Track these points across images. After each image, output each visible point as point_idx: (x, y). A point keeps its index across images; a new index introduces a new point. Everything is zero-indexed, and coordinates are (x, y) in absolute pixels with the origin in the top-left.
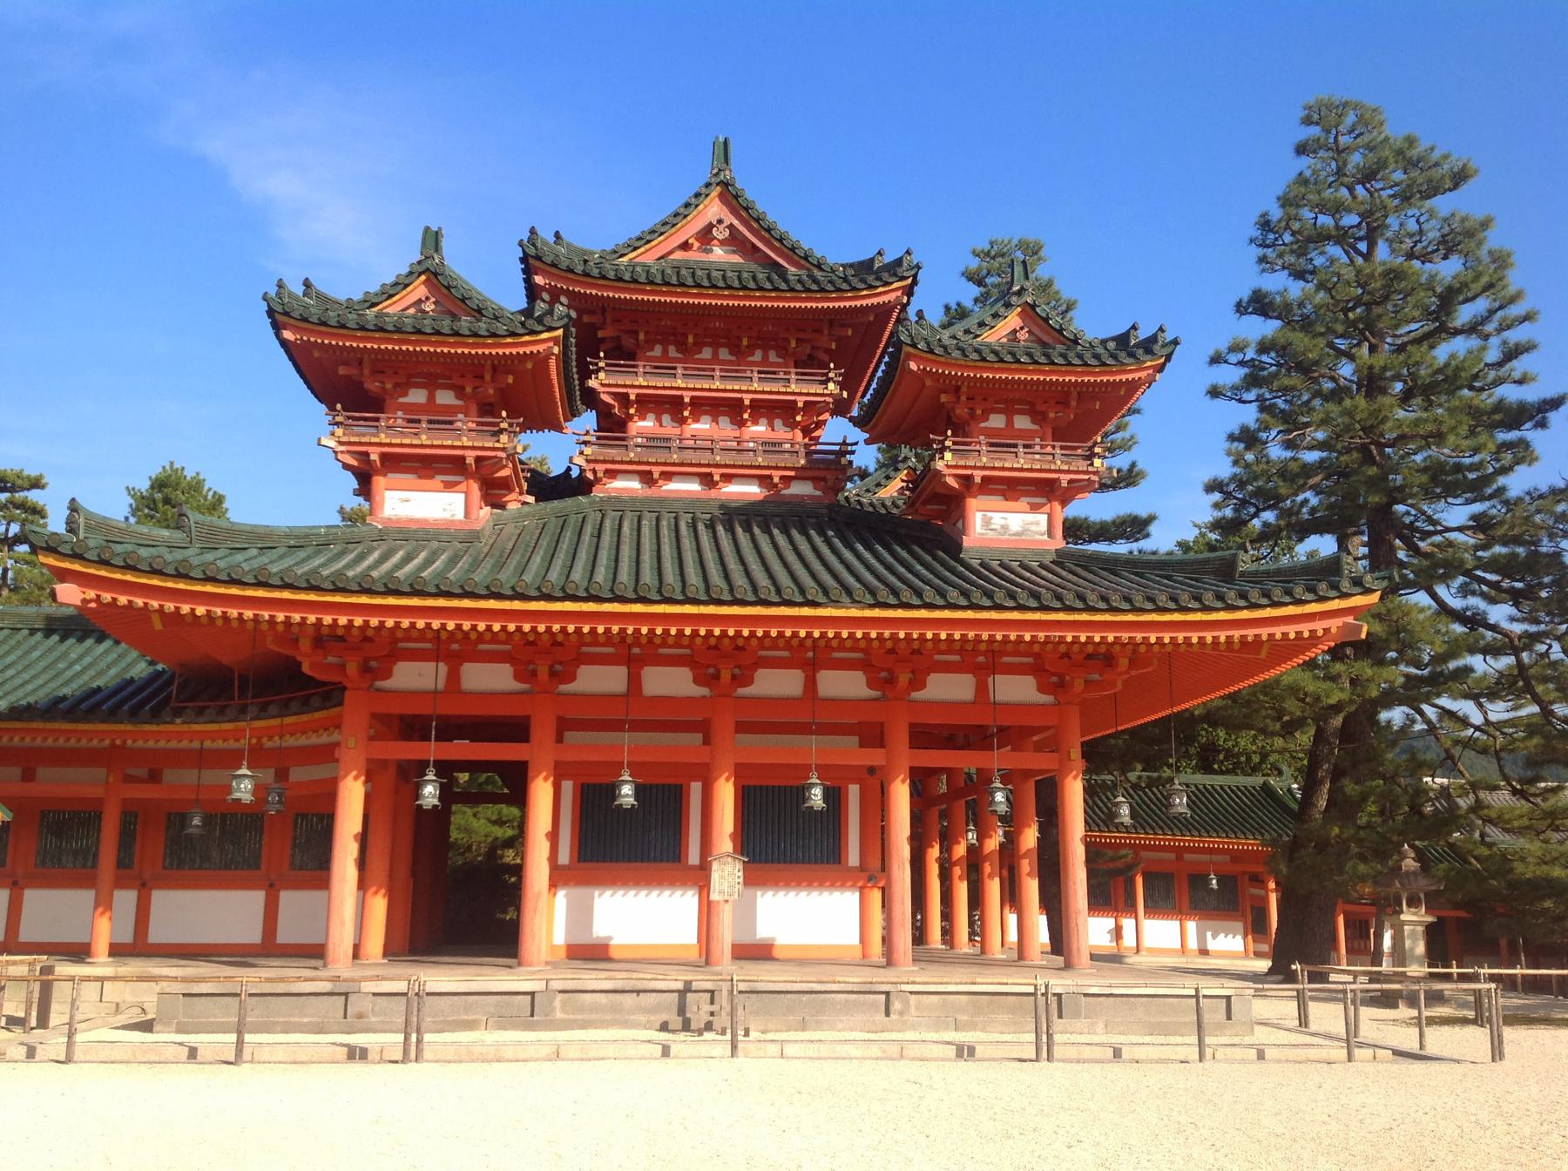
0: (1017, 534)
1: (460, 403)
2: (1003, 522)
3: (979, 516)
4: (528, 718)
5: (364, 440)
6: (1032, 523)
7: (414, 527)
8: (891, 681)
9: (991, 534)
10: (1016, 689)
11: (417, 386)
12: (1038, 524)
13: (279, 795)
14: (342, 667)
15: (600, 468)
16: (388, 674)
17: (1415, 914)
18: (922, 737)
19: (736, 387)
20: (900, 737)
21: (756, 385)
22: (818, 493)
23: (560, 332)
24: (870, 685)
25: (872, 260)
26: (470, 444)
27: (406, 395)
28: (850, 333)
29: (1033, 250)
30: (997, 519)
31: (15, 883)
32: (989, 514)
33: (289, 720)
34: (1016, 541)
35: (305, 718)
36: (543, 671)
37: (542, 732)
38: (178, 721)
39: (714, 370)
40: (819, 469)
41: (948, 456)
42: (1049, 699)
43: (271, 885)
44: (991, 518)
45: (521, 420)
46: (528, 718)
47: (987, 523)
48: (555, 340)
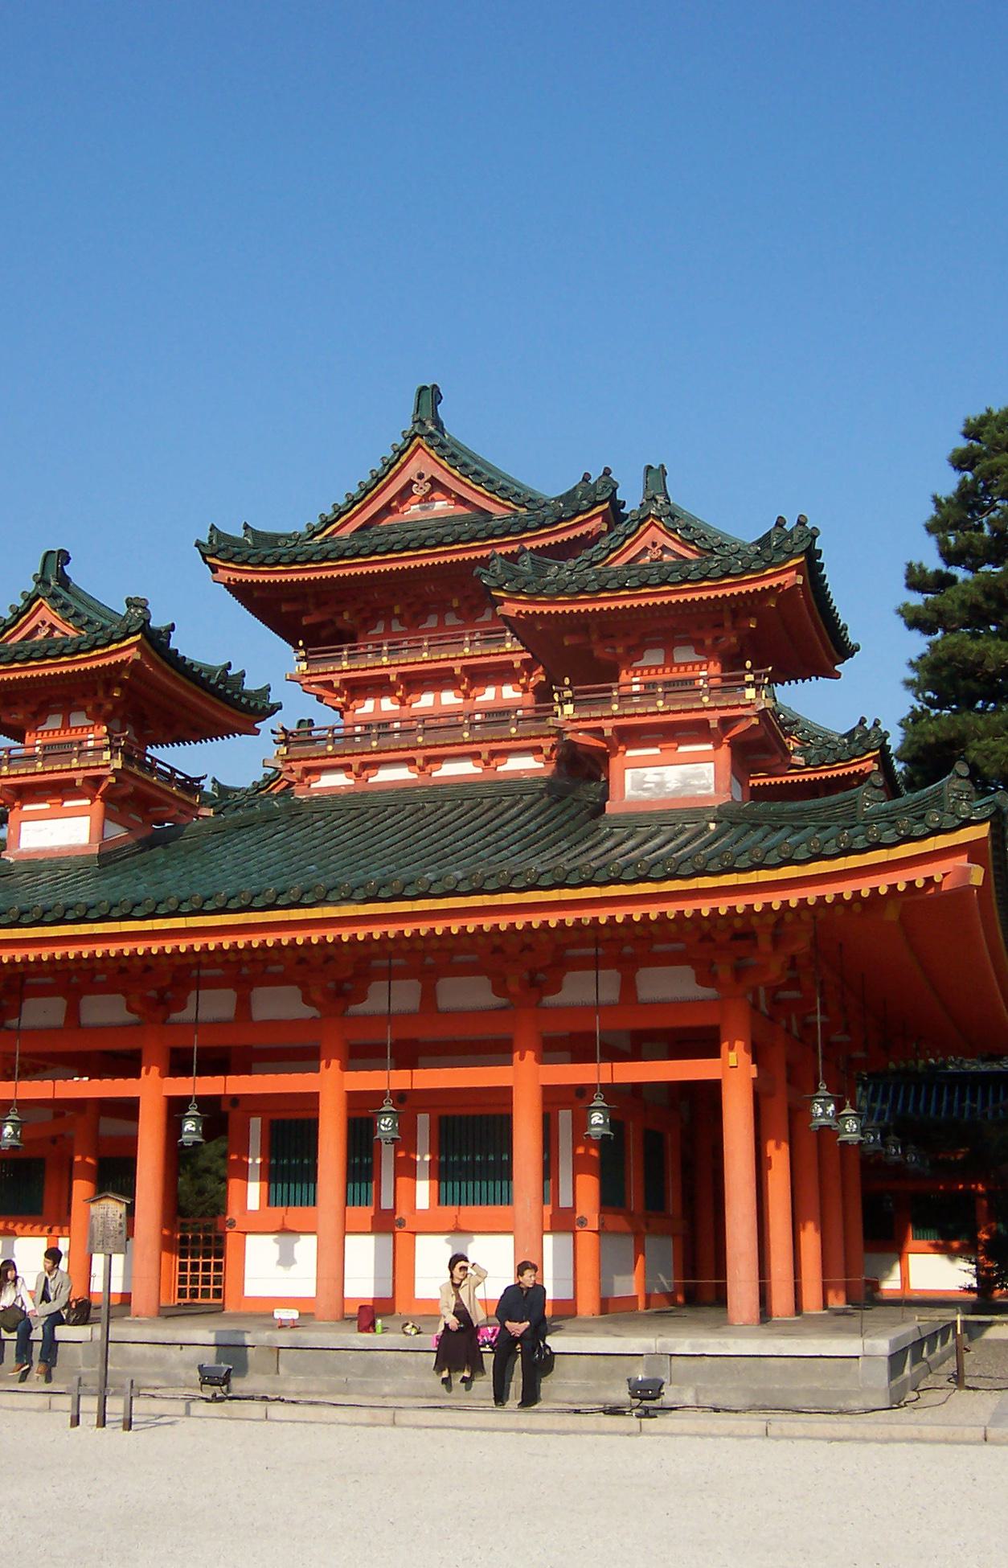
0: (674, 791)
2: (657, 778)
3: (628, 773)
6: (694, 776)
12: (701, 776)
15: (298, 766)
30: (650, 774)
39: (381, 645)
45: (770, 669)
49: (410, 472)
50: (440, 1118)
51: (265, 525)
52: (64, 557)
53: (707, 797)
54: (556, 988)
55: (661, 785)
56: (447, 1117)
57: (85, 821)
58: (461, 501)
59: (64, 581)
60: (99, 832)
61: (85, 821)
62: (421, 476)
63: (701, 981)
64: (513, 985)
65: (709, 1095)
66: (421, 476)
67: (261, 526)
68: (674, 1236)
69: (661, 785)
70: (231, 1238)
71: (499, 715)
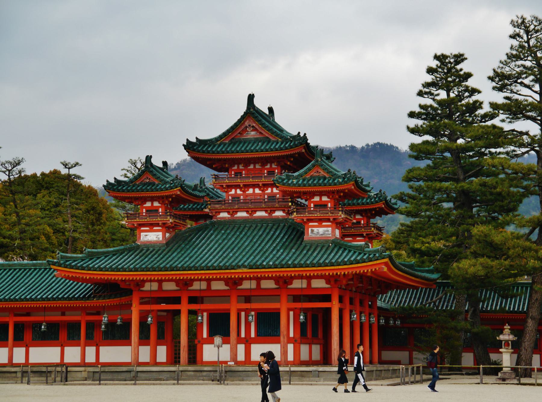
0: (322, 235)
2: (317, 231)
3: (310, 229)
4: (180, 297)
5: (133, 221)
6: (326, 231)
7: (148, 243)
9: (314, 236)
10: (319, 284)
11: (149, 201)
12: (328, 231)
13: (121, 320)
17: (507, 349)
19: (257, 181)
21: (263, 179)
22: (284, 214)
26: (160, 220)
30: (315, 229)
31: (62, 345)
32: (313, 229)
34: (320, 237)
37: (184, 301)
38: (95, 299)
40: (282, 207)
41: (295, 214)
46: (180, 297)
47: (312, 231)
49: (247, 124)
50: (257, 313)
51: (202, 137)
52: (151, 157)
53: (329, 237)
54: (291, 284)
55: (318, 233)
56: (259, 313)
57: (161, 233)
58: (261, 133)
59: (152, 164)
60: (164, 236)
61: (161, 233)
62: (249, 125)
63: (327, 283)
64: (281, 283)
65: (328, 312)
66: (249, 125)
67: (201, 138)
68: (320, 344)
69: (318, 233)
70: (198, 346)
71: (272, 197)
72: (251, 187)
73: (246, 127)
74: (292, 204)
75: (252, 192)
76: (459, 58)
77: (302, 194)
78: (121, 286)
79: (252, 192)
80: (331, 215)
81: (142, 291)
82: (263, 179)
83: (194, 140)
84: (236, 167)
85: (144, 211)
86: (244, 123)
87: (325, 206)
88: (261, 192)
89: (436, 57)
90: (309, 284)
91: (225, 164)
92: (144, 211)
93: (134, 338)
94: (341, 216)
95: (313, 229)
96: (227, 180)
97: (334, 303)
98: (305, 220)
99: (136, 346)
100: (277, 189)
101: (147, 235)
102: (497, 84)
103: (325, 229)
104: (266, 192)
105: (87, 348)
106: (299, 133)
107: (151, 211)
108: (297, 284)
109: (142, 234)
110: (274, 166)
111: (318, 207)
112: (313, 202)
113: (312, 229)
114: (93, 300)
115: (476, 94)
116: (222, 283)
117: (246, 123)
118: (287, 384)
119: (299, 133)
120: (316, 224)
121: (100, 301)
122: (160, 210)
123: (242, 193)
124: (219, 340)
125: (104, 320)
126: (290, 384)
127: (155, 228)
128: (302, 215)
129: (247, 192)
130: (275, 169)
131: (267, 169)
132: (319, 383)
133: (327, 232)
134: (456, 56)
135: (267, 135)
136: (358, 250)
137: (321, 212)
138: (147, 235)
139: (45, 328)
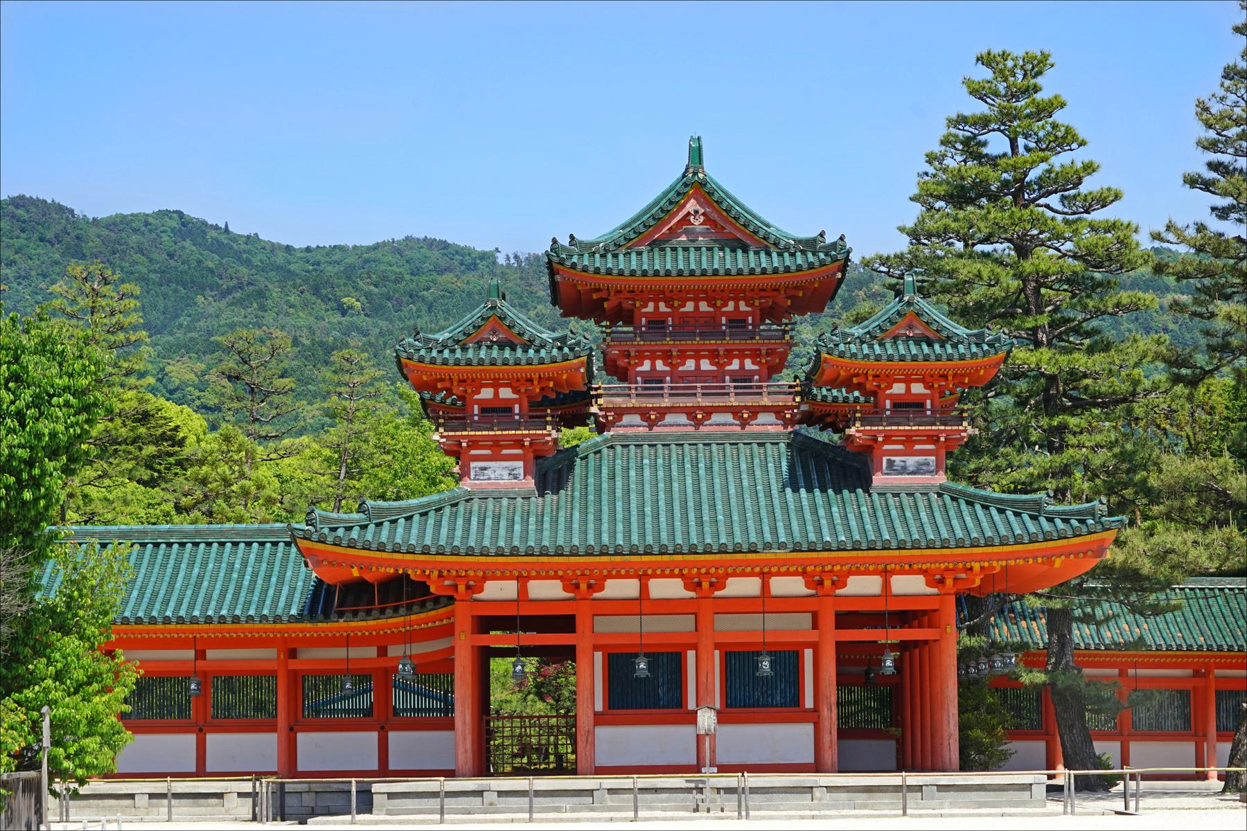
1: (516, 396)
2: (902, 464)
3: (885, 459)
4: (574, 616)
6: (924, 464)
8: (821, 583)
10: (909, 585)
12: (928, 464)
14: (456, 587)
16: (481, 590)
18: (846, 619)
20: (829, 621)
23: (585, 358)
24: (807, 586)
25: (814, 240)
27: (479, 393)
28: (801, 295)
29: (1037, 65)
30: (897, 459)
32: (893, 458)
33: (413, 617)
35: (422, 615)
36: (583, 586)
38: (341, 620)
41: (858, 424)
42: (934, 591)
43: (383, 728)
44: (894, 461)
46: (574, 616)
47: (891, 463)
48: (582, 364)
66: (696, 212)
72: (691, 357)
73: (689, 214)
74: (802, 400)
75: (693, 368)
76: (1037, 65)
77: (870, 378)
78: (432, 589)
79: (693, 368)
80: (942, 428)
81: (476, 600)
82: (728, 338)
83: (564, 241)
84: (650, 307)
85: (476, 412)
86: (684, 205)
87: (916, 405)
88: (714, 368)
89: (986, 60)
90: (886, 585)
91: (634, 300)
92: (476, 412)
93: (463, 712)
94: (965, 431)
95: (893, 458)
96: (638, 339)
97: (949, 630)
98: (880, 439)
99: (467, 732)
100: (753, 363)
101: (485, 469)
102: (1218, 134)
103: (921, 459)
104: (728, 368)
105: (301, 737)
106: (822, 235)
107: (493, 410)
108: (863, 586)
109: (473, 464)
110: (743, 307)
111: (911, 409)
112: (891, 396)
113: (888, 460)
114: (338, 621)
115: (1074, 146)
116: (679, 582)
117: (688, 206)
118: (896, 816)
119: (822, 235)
120: (900, 447)
121: (353, 624)
122: (517, 409)
123: (667, 369)
124: (710, 717)
125: (404, 670)
126: (905, 814)
127: (505, 452)
128: (876, 428)
129: (681, 368)
130: (747, 314)
131: (725, 314)
132: (943, 811)
133: (925, 468)
134: (1028, 58)
135: (739, 235)
136: (1026, 509)
137: (918, 420)
138: (485, 469)
139: (198, 689)
